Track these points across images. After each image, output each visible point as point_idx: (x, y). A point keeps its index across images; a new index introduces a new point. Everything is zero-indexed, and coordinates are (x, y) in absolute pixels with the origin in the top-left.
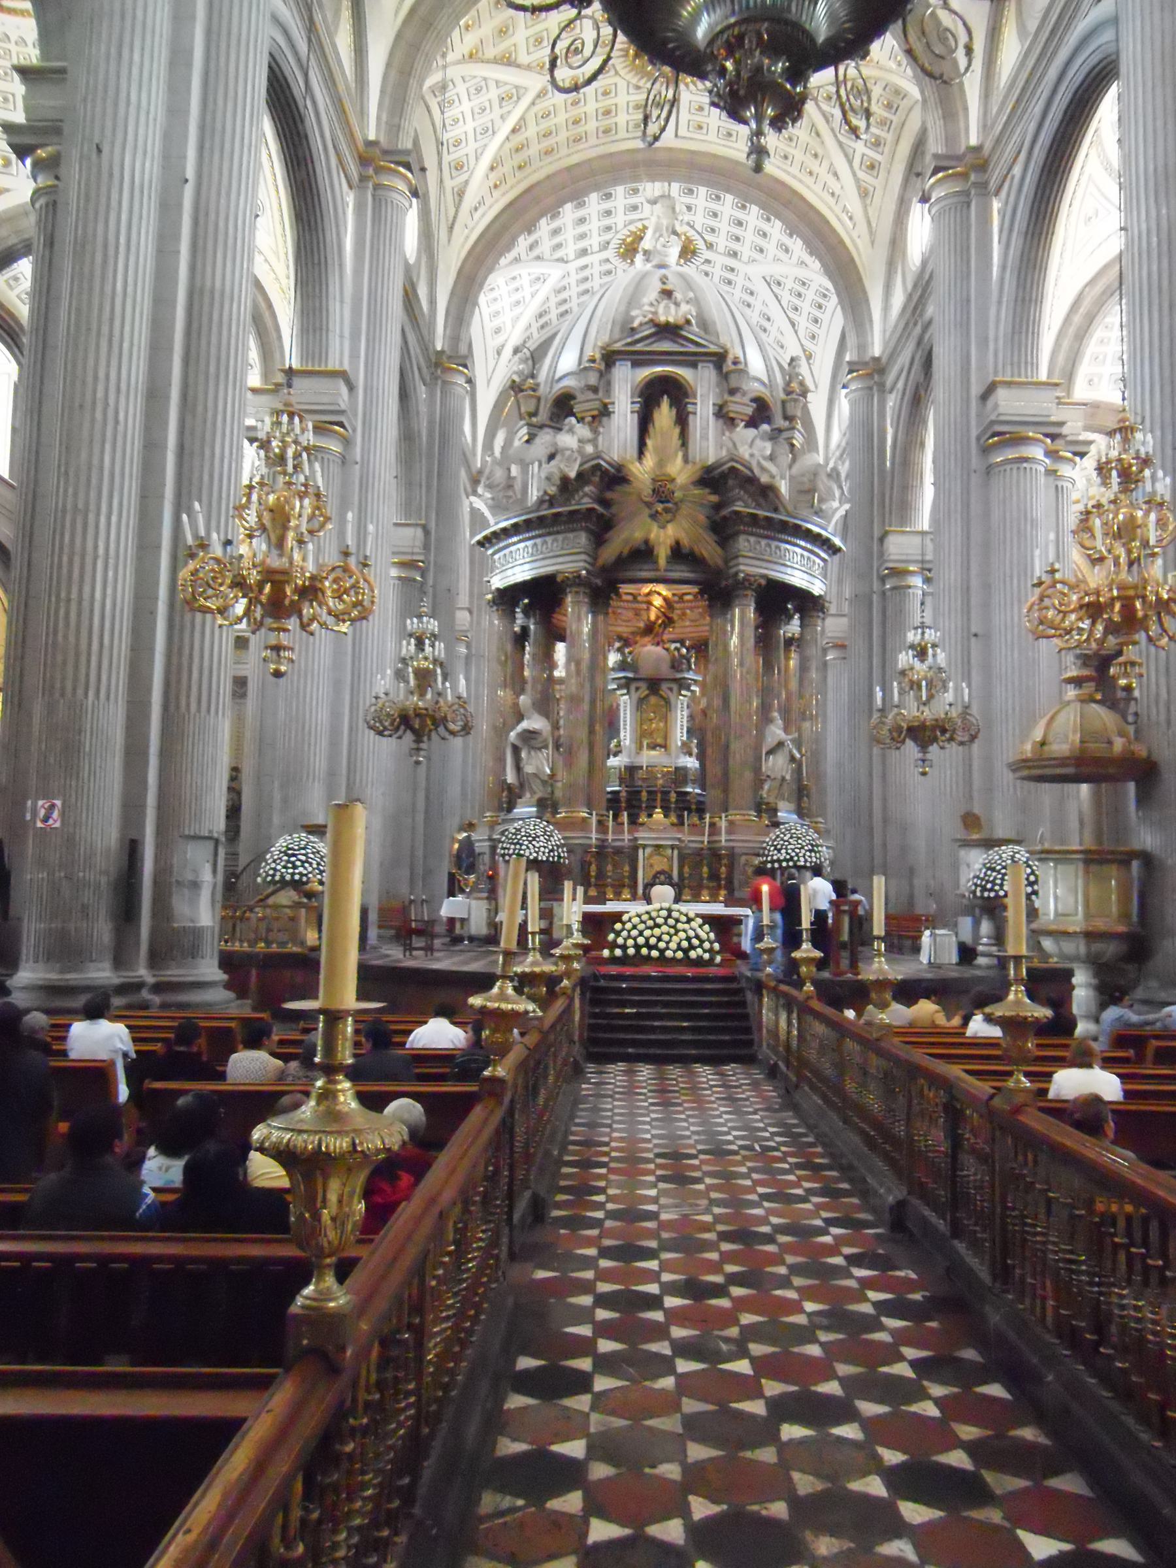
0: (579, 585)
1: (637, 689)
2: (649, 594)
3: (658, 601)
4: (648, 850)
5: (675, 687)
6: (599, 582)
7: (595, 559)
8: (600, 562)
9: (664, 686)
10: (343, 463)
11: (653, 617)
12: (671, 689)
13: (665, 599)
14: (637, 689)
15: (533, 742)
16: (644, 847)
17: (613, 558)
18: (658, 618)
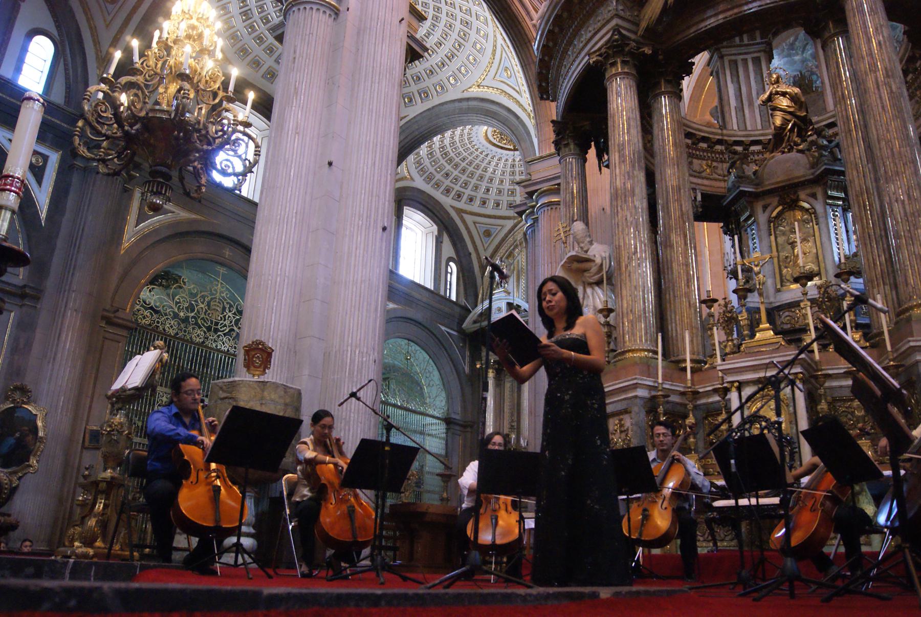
0: (616, 54)
1: (765, 208)
2: (770, 99)
3: (784, 103)
4: (747, 391)
5: (819, 191)
6: (648, 50)
7: (638, 25)
8: (644, 25)
9: (802, 195)
10: (337, 14)
11: (778, 122)
12: (814, 196)
13: (793, 98)
14: (765, 208)
15: (586, 274)
16: (740, 386)
17: (658, 11)
18: (785, 122)
